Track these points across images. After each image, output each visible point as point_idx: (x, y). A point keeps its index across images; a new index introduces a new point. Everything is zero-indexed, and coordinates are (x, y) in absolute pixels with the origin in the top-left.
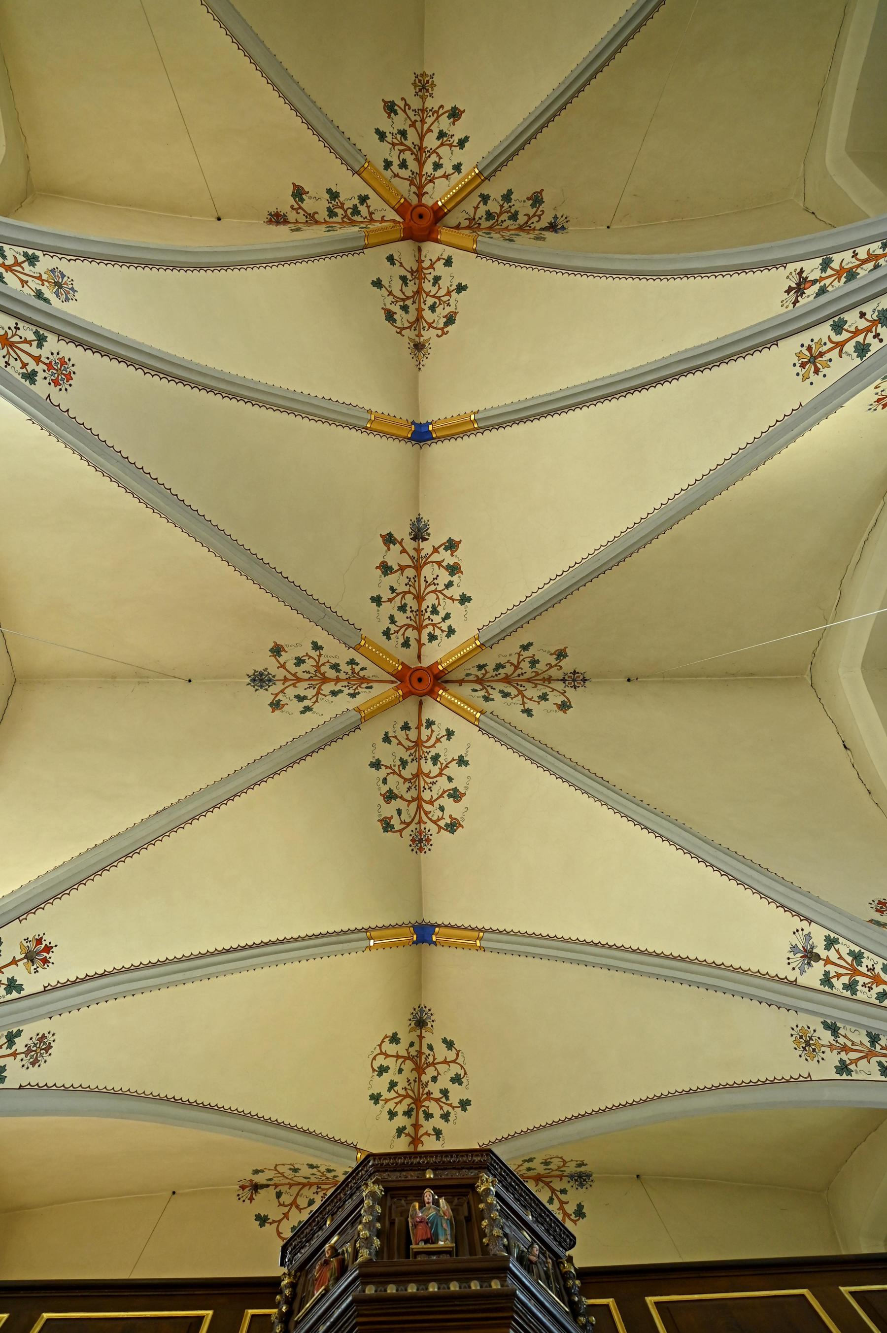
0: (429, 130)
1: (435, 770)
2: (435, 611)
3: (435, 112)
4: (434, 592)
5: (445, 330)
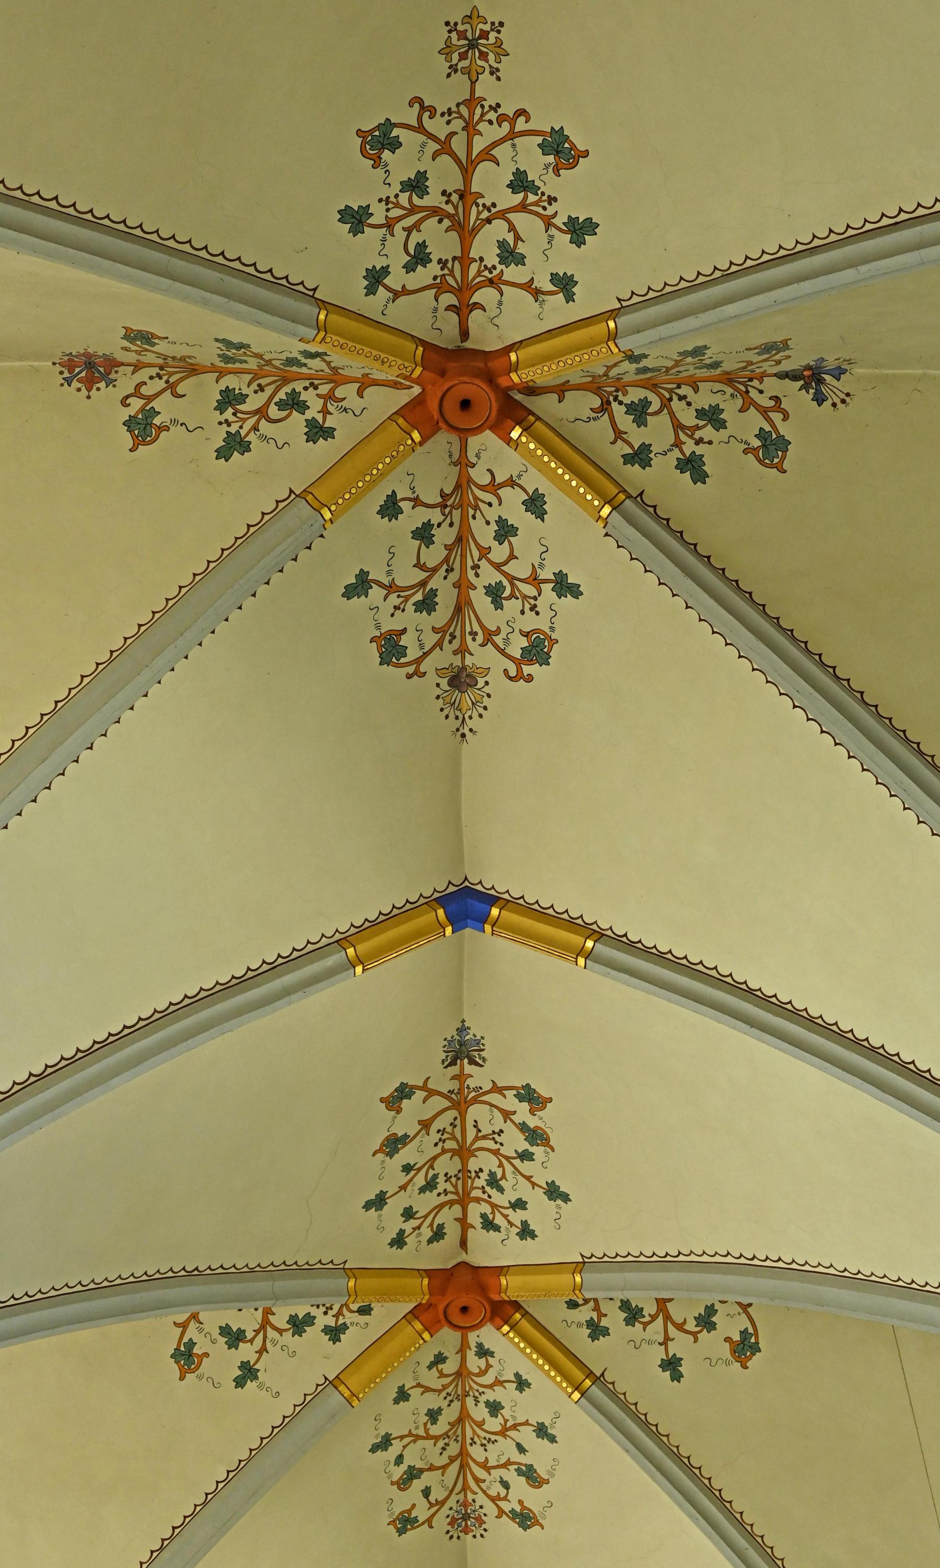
0: (487, 155)
1: (494, 1424)
2: (494, 1182)
3: (501, 119)
4: (496, 1153)
5: (527, 669)
